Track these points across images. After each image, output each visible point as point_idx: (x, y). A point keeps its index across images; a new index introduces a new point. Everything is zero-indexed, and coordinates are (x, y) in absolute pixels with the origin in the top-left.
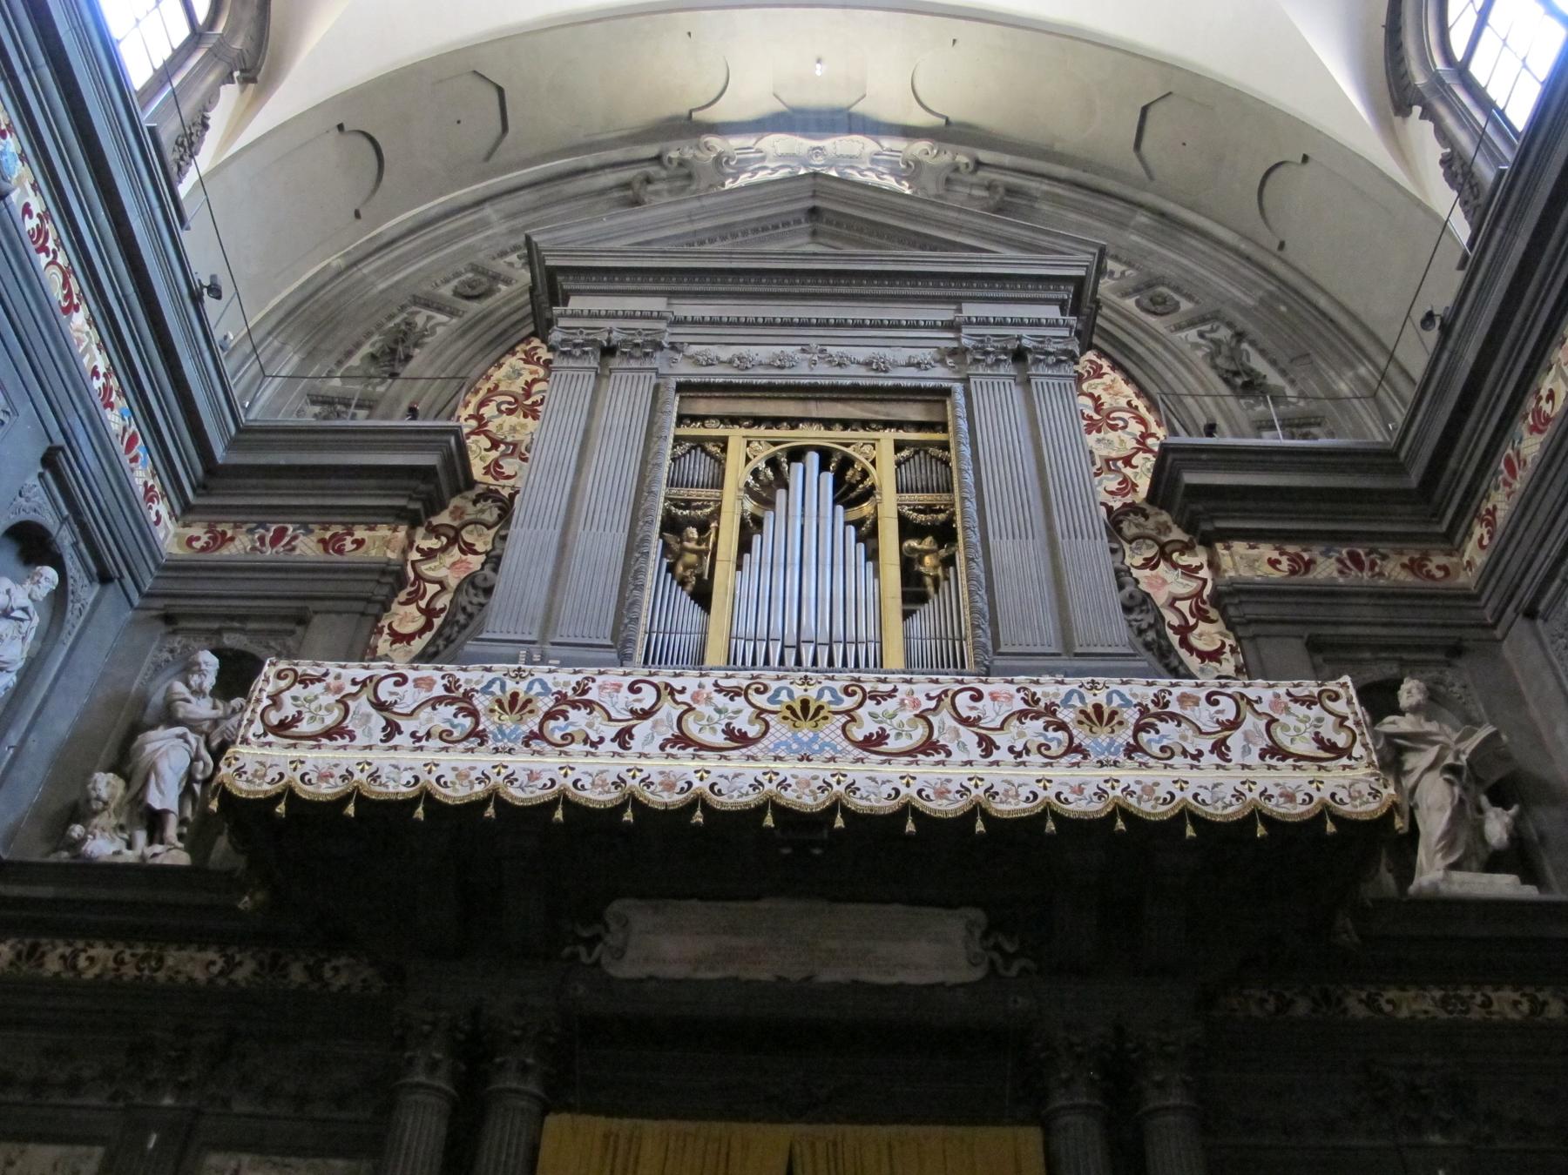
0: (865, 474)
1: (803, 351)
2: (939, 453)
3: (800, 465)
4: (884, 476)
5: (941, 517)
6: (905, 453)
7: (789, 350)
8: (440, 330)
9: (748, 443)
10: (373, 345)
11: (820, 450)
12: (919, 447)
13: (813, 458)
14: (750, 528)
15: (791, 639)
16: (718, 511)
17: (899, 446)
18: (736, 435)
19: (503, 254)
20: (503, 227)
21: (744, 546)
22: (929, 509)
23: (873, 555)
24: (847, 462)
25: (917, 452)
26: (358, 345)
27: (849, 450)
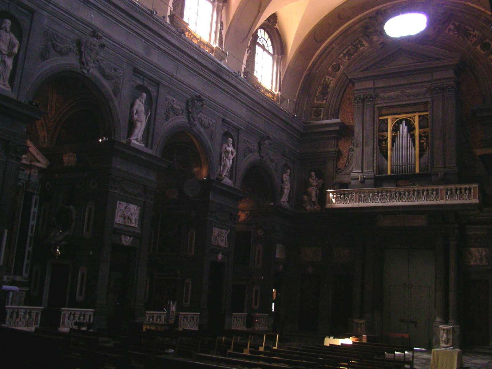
0: (414, 124)
1: (400, 93)
2: (427, 117)
3: (401, 125)
4: (417, 125)
5: (427, 134)
6: (421, 118)
7: (398, 93)
8: (332, 82)
9: (392, 119)
10: (320, 89)
11: (406, 120)
12: (423, 116)
13: (404, 122)
14: (393, 141)
15: (401, 165)
16: (388, 137)
17: (420, 116)
18: (390, 118)
19: (339, 55)
20: (337, 47)
21: (392, 146)
22: (424, 133)
23: (414, 145)
24: (410, 121)
25: (423, 118)
26: (317, 90)
27: (410, 119)
